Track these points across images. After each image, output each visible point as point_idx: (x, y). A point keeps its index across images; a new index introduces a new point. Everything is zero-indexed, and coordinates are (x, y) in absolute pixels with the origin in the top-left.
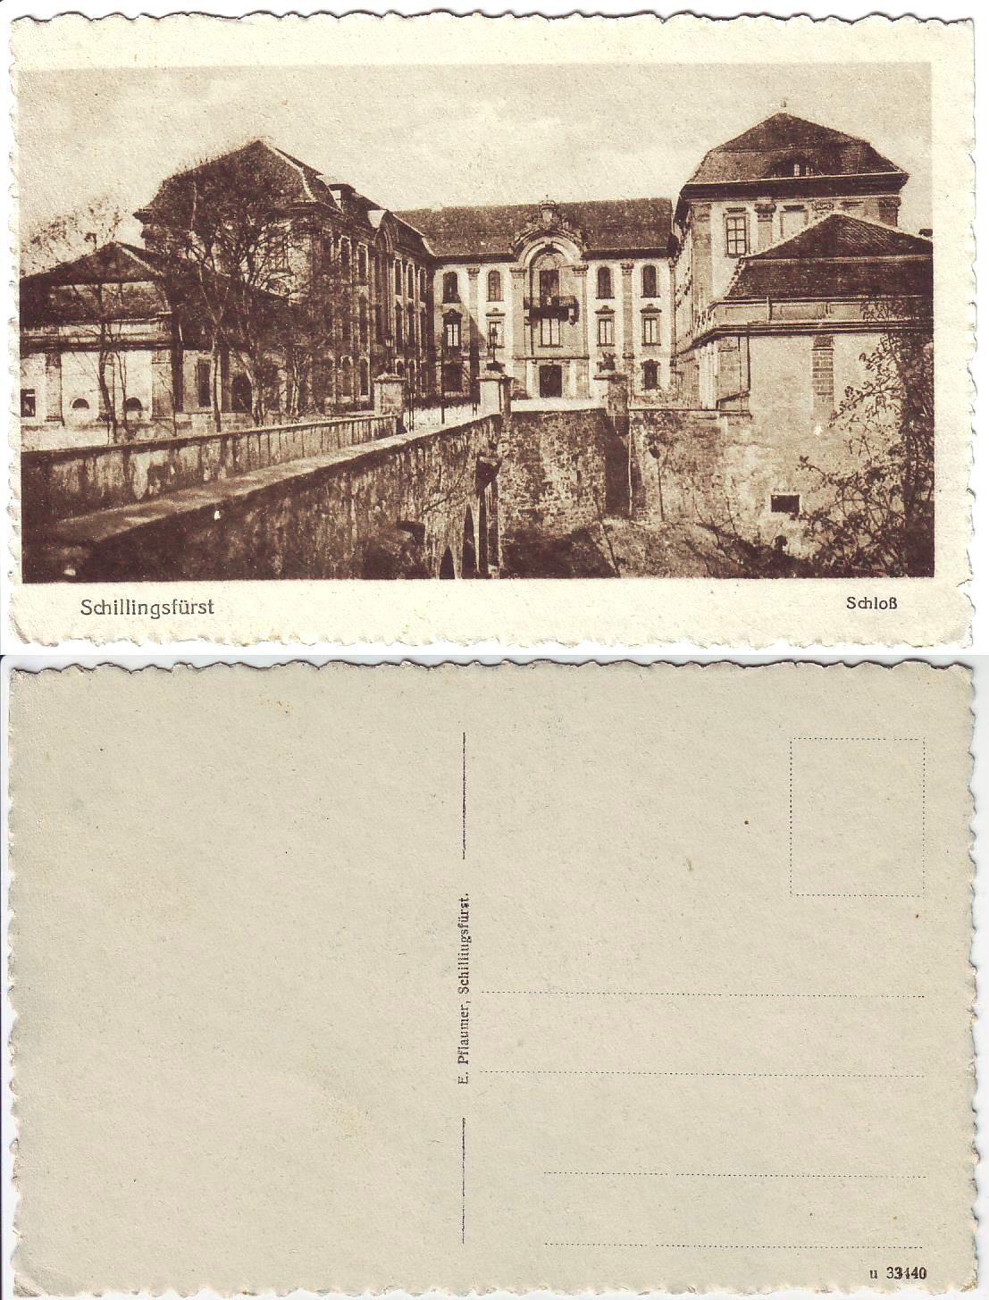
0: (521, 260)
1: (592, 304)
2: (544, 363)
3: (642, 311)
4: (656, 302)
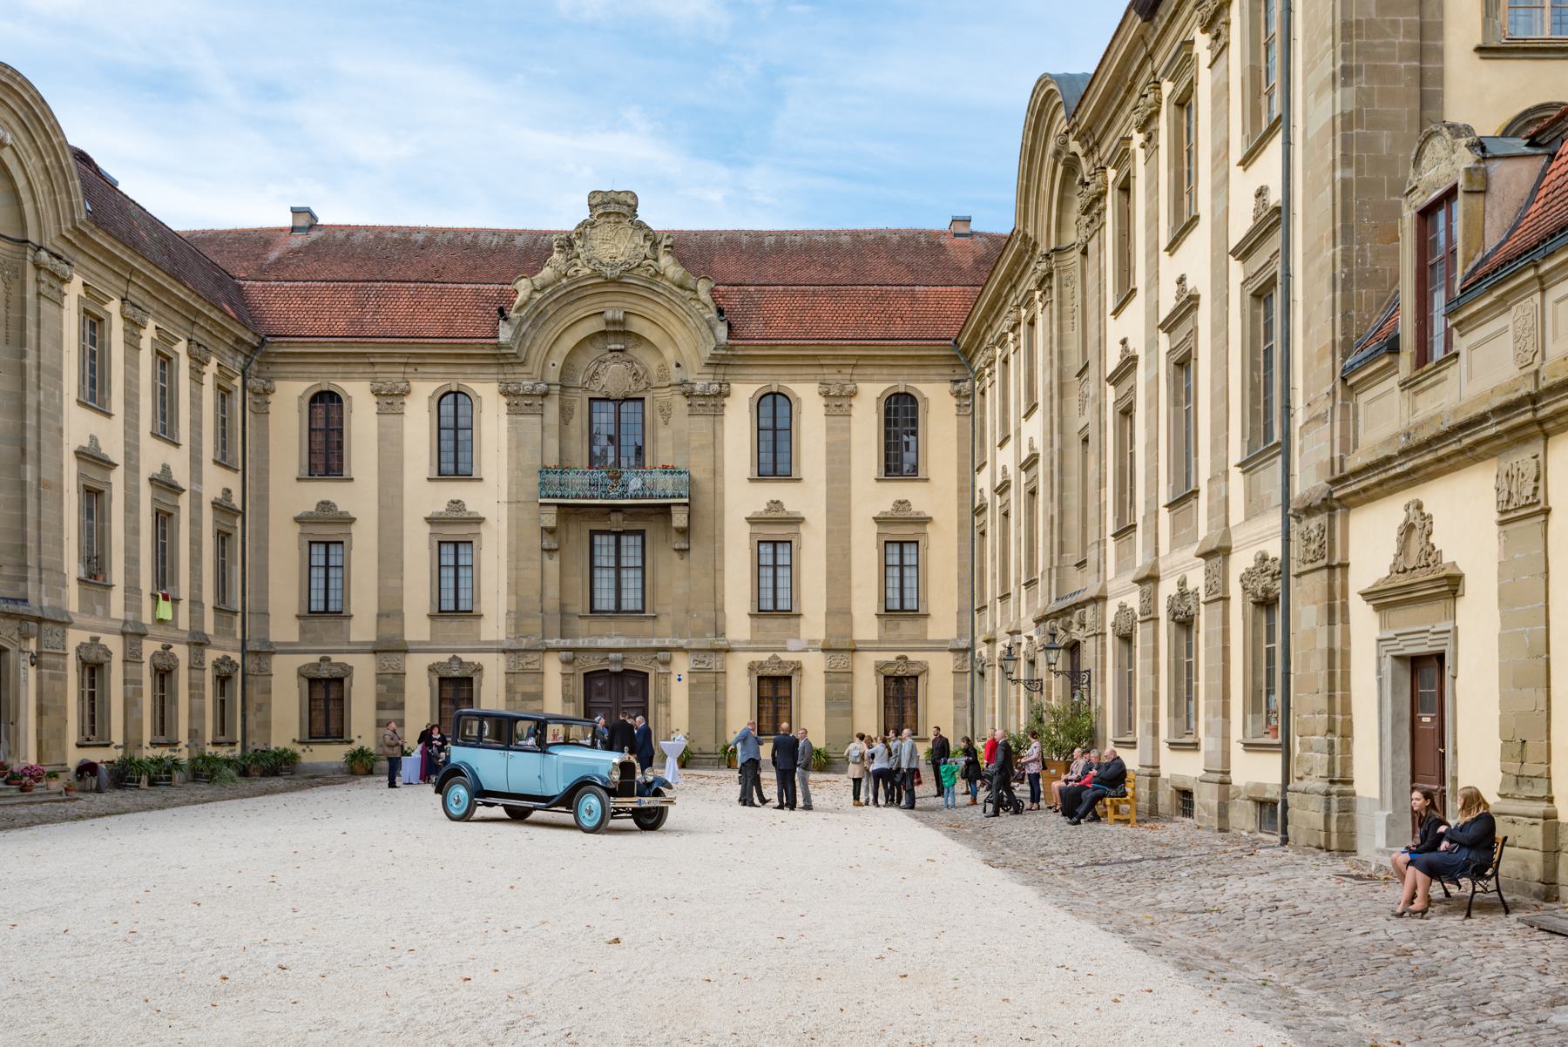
0: (534, 366)
1: (742, 499)
2: (594, 664)
3: (877, 520)
4: (916, 496)
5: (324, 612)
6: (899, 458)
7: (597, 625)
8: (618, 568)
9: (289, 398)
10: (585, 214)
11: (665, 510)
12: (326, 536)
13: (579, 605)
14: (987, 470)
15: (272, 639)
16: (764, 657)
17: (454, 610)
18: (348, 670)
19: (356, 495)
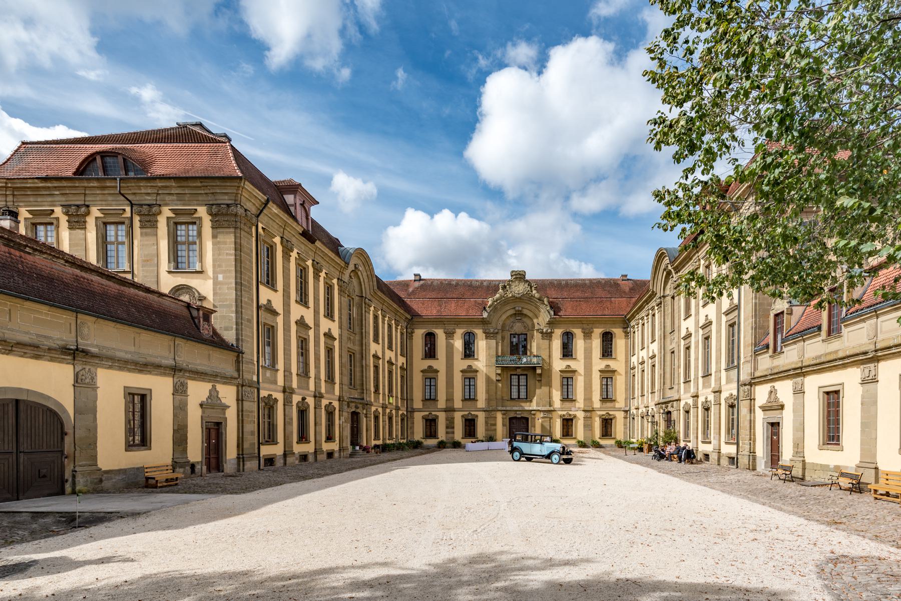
0: (494, 325)
1: (558, 364)
2: (512, 415)
5: (430, 399)
6: (607, 352)
7: (512, 403)
8: (519, 386)
9: (419, 334)
10: (509, 278)
11: (534, 368)
12: (430, 375)
13: (507, 397)
14: (635, 356)
15: (415, 407)
16: (564, 413)
17: (469, 398)
18: (437, 417)
19: (440, 364)
